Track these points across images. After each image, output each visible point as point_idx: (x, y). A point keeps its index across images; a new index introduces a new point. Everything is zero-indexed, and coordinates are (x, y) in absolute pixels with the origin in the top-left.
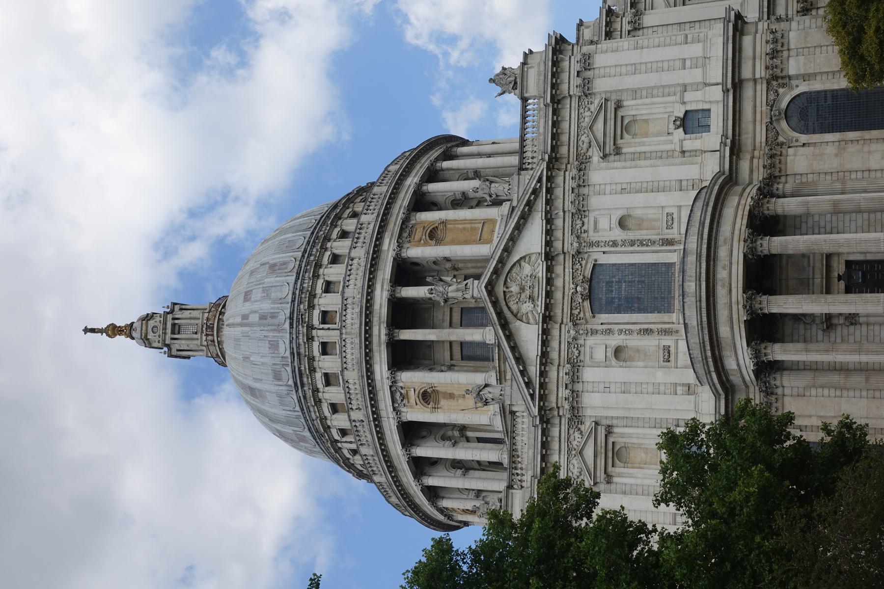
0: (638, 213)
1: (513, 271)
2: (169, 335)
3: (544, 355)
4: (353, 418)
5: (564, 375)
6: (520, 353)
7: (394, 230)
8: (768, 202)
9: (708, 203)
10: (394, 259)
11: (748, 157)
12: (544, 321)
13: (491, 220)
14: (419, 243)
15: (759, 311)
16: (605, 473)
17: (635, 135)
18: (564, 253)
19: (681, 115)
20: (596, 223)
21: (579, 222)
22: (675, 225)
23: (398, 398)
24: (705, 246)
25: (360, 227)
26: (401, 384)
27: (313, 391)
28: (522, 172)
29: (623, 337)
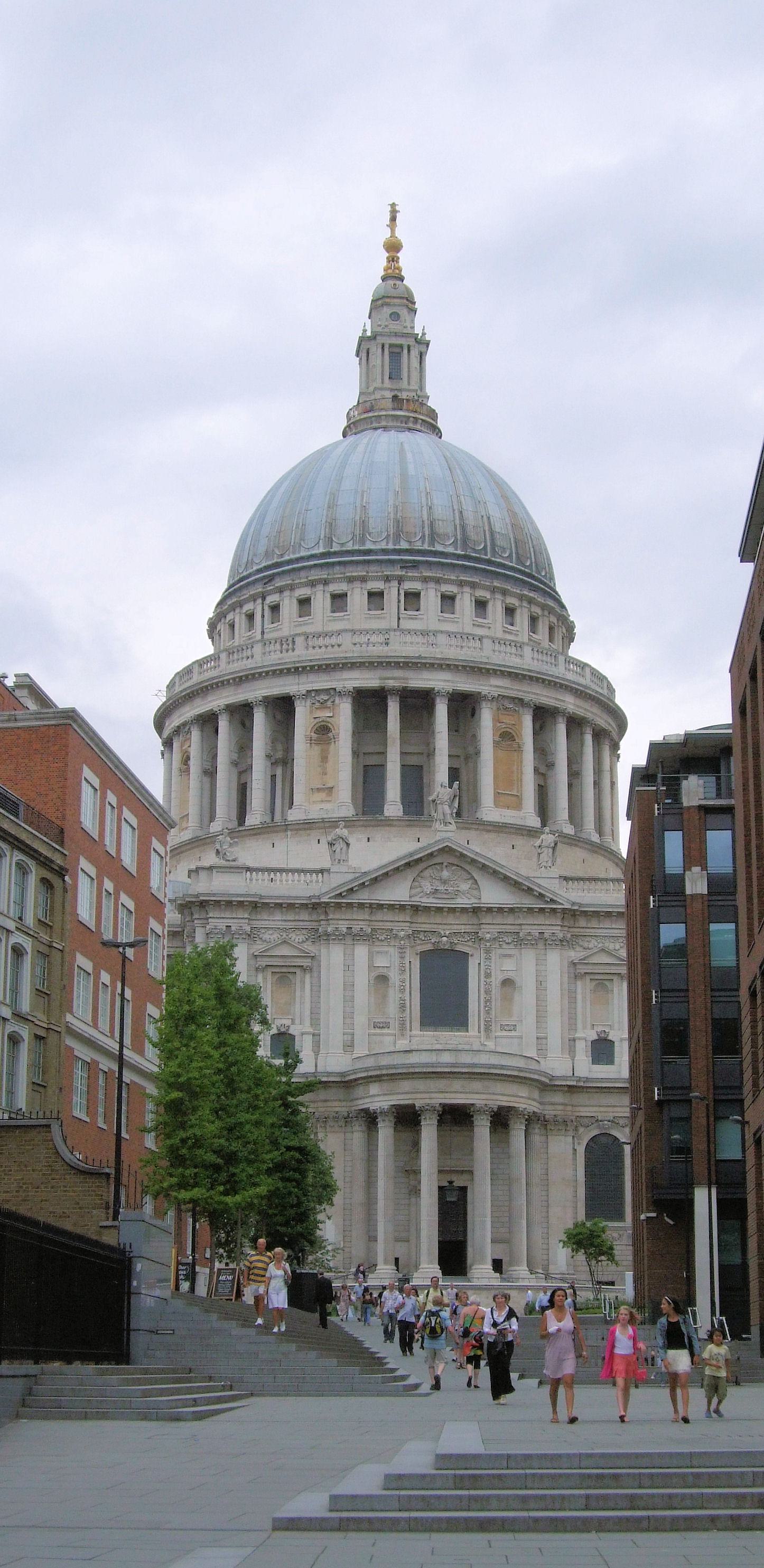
0: (517, 997)
2: (388, 341)
3: (380, 906)
4: (297, 639)
5: (360, 927)
6: (381, 880)
8: (521, 1123)
9: (522, 1071)
10: (480, 693)
12: (412, 906)
13: (521, 804)
14: (496, 720)
17: (594, 991)
19: (610, 1038)
20: (510, 956)
22: (505, 1033)
23: (322, 697)
24: (482, 1071)
26: (337, 701)
29: (398, 983)
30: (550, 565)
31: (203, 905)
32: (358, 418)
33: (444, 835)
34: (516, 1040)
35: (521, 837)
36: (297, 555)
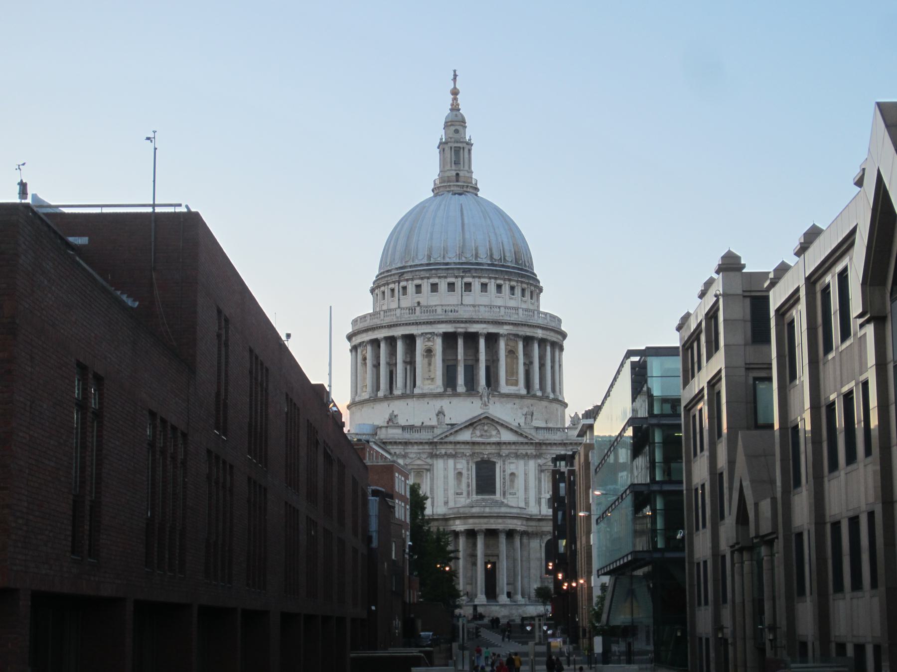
0: (516, 481)
1: (494, 427)
3: (459, 443)
4: (416, 308)
7: (514, 330)
10: (498, 333)
11: (537, 525)
12: (472, 442)
15: (478, 534)
16: (412, 469)
18: (500, 449)
20: (513, 463)
21: (513, 456)
22: (511, 496)
25: (516, 309)
26: (435, 338)
27: (428, 277)
28: (535, 430)
29: (466, 476)
30: (531, 258)
31: (384, 443)
32: (439, 185)
33: (485, 411)
34: (516, 499)
35: (517, 399)
36: (415, 264)
